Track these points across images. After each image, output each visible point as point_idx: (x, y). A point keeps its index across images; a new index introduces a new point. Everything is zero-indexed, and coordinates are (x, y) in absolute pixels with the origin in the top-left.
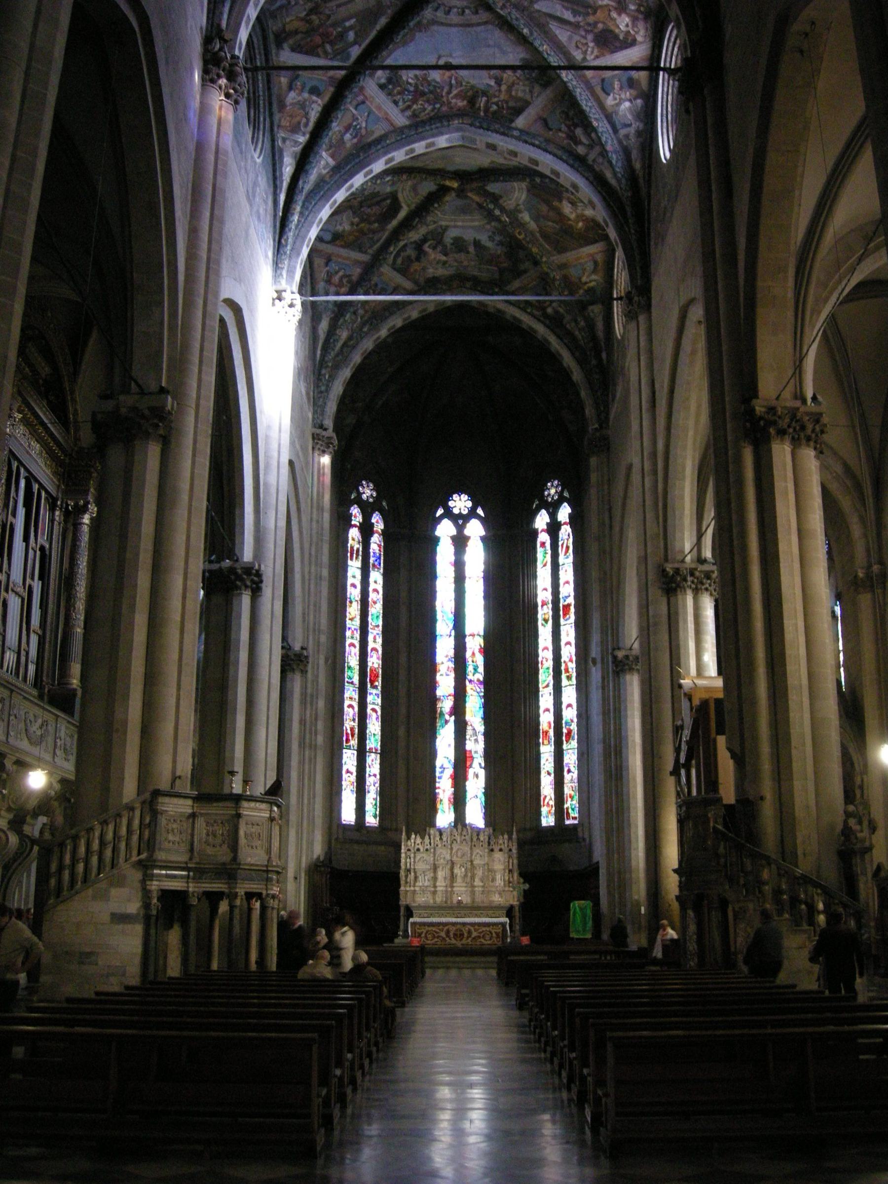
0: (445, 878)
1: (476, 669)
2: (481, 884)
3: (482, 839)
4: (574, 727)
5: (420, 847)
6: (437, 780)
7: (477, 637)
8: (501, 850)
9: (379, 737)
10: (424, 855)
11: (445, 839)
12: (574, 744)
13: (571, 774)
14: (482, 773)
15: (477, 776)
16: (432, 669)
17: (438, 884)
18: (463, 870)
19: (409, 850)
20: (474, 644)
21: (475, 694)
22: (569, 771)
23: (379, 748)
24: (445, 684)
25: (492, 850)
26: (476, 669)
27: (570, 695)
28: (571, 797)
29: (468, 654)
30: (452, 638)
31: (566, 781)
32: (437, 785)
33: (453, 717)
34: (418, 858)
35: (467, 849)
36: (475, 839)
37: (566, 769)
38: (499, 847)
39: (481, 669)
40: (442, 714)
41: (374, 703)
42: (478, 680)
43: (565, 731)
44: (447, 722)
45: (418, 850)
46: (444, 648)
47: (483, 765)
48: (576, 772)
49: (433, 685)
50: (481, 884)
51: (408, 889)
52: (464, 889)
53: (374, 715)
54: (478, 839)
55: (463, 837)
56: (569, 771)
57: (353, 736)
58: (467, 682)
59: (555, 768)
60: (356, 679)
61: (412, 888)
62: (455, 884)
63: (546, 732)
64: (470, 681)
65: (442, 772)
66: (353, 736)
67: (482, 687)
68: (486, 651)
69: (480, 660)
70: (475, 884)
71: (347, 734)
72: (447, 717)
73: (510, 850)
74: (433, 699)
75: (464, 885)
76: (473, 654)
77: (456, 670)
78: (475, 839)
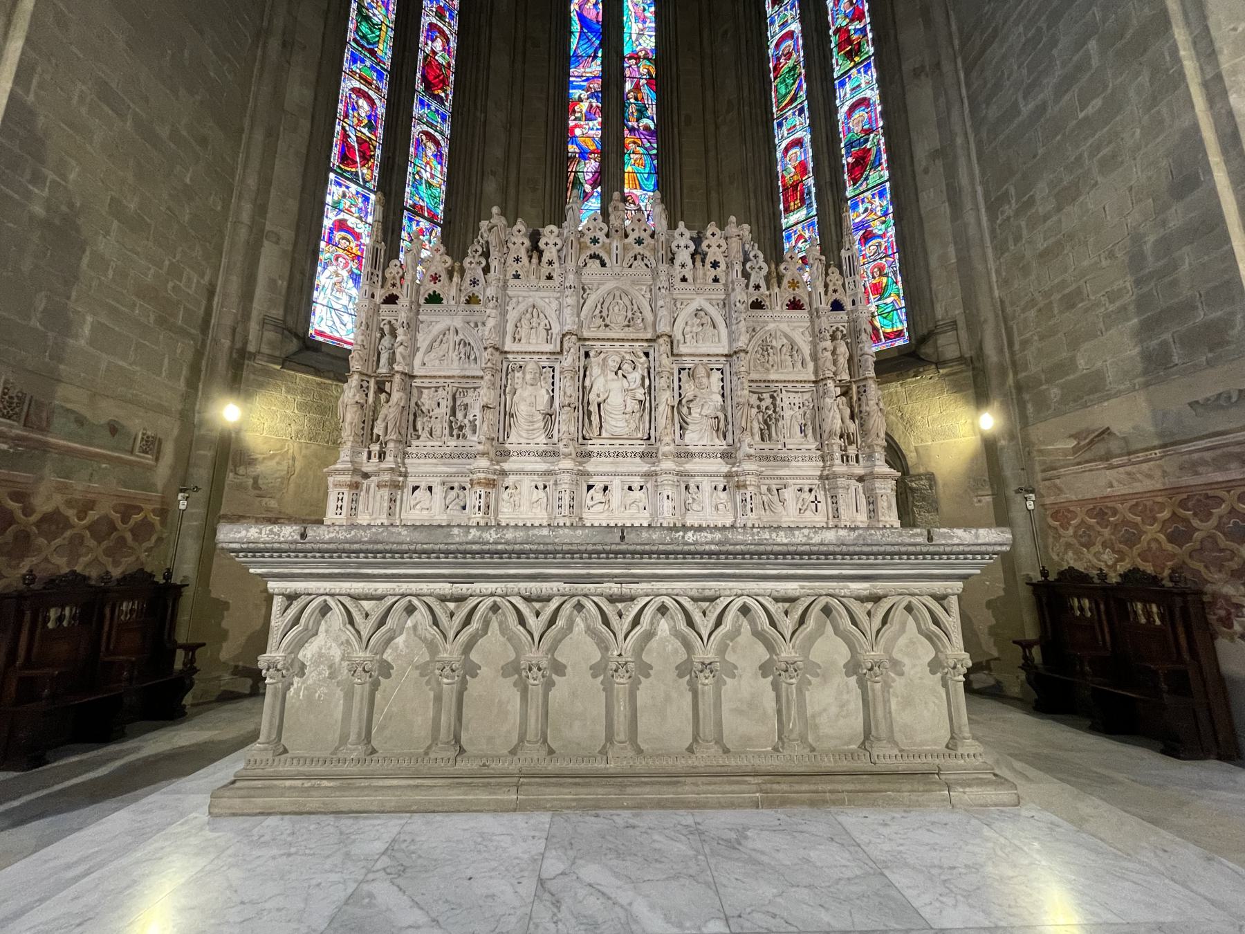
0: (549, 416)
1: (642, 112)
2: (720, 444)
3: (714, 254)
4: (877, 141)
7: (644, 63)
8: (795, 305)
9: (441, 192)
10: (458, 322)
11: (550, 253)
12: (880, 175)
16: (564, 106)
17: (516, 439)
18: (635, 377)
20: (638, 73)
21: (641, 150)
22: (867, 238)
23: (441, 215)
24: (587, 131)
25: (757, 305)
26: (642, 112)
27: (859, 85)
29: (628, 86)
30: (599, 61)
33: (599, 189)
36: (684, 256)
38: (788, 295)
39: (652, 111)
40: (577, 183)
41: (431, 125)
42: (647, 128)
43: (847, 160)
44: (586, 196)
46: (586, 71)
48: (892, 231)
49: (565, 135)
53: (431, 148)
57: (366, 158)
58: (626, 132)
60: (385, 50)
62: (594, 446)
63: (795, 186)
64: (632, 130)
66: (366, 158)
67: (654, 140)
68: (657, 83)
69: (649, 95)
70: (690, 437)
71: (345, 146)
72: (588, 188)
74: (565, 160)
75: (641, 447)
76: (637, 88)
77: (604, 111)
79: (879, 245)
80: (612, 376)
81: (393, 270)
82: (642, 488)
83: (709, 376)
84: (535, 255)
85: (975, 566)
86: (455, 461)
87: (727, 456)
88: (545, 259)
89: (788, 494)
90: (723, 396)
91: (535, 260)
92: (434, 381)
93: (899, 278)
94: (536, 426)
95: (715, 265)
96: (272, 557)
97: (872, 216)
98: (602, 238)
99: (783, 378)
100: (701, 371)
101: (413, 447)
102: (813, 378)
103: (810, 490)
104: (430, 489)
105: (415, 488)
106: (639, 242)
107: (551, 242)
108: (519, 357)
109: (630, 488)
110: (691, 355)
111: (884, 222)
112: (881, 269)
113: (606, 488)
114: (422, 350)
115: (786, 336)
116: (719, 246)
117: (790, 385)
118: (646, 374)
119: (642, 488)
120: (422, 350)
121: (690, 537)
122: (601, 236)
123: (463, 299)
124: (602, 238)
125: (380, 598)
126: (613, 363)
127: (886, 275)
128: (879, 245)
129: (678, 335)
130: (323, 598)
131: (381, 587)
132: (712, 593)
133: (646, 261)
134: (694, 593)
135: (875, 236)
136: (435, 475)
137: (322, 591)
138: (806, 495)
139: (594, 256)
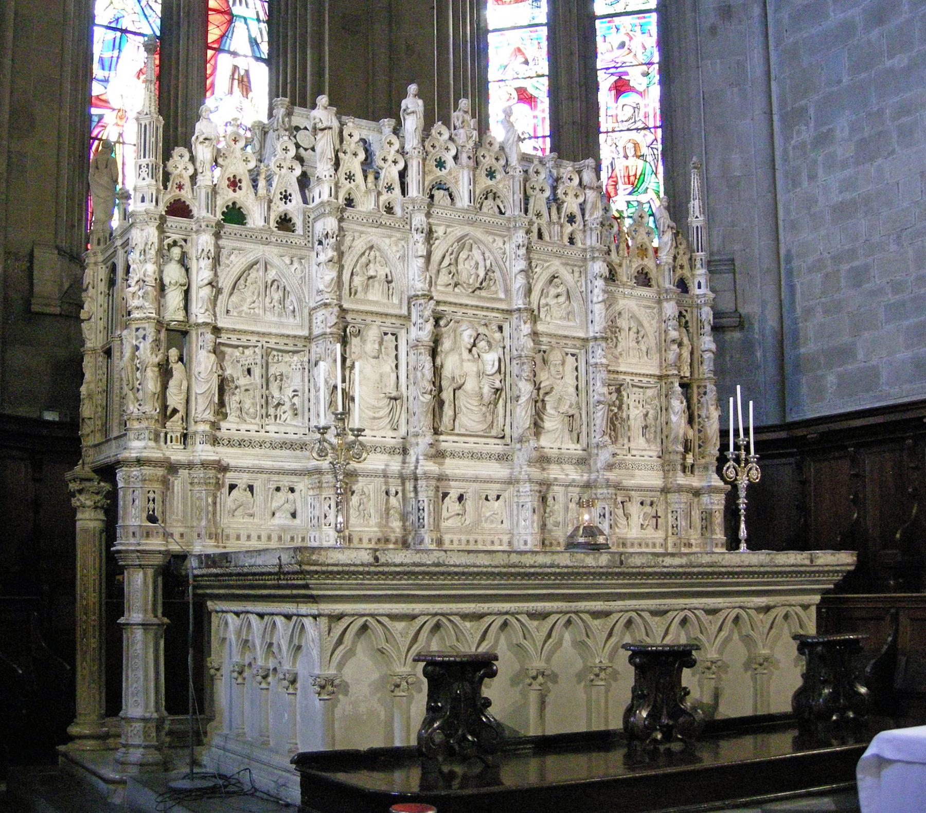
3: (571, 205)
5: (245, 197)
6: (97, 71)
8: (643, 279)
13: (629, 99)
14: (261, 75)
15: (244, 83)
18: (491, 358)
19: (179, 209)
22: (621, 87)
28: (635, 182)
31: (605, 123)
32: (97, 89)
34: (234, 263)
35: (509, 251)
36: (539, 201)
37: (605, 81)
45: (235, 215)
47: (265, 48)
48: (655, 92)
50: (574, 448)
51: (176, 453)
52: (498, 471)
54: (555, 201)
55: (485, 182)
56: (621, 87)
59: (554, 76)
61: (203, 452)
62: (447, 443)
65: (117, 46)
73: (683, 285)
78: (539, 201)
79: (636, 108)
80: (466, 355)
81: (179, 163)
82: (498, 497)
83: (563, 363)
84: (371, 178)
85: (830, 582)
86: (278, 452)
87: (582, 462)
88: (382, 183)
89: (634, 509)
90: (577, 388)
91: (371, 178)
92: (244, 338)
93: (661, 169)
94: (381, 414)
95: (571, 219)
96: (356, 579)
97: (629, 59)
98: (450, 163)
99: (630, 370)
100: (555, 357)
101: (223, 430)
102: (657, 373)
103: (652, 504)
104: (251, 488)
105: (232, 487)
106: (491, 174)
107: (390, 158)
108: (359, 319)
109: (487, 499)
110: (550, 335)
111: (646, 74)
112: (636, 146)
113: (461, 498)
114: (226, 292)
115: (633, 317)
116: (576, 196)
117: (636, 379)
118: (502, 357)
119: (498, 497)
120: (226, 292)
121: (668, 561)
122: (448, 157)
123: (273, 224)
124: (450, 163)
125: (413, 617)
126: (467, 337)
127: (641, 157)
128: (636, 108)
129: (535, 307)
130: (365, 619)
131: (417, 608)
132: (666, 608)
133: (498, 202)
134: (653, 608)
135: (633, 90)
136: (261, 471)
137: (367, 612)
138: (647, 509)
139: (440, 186)
